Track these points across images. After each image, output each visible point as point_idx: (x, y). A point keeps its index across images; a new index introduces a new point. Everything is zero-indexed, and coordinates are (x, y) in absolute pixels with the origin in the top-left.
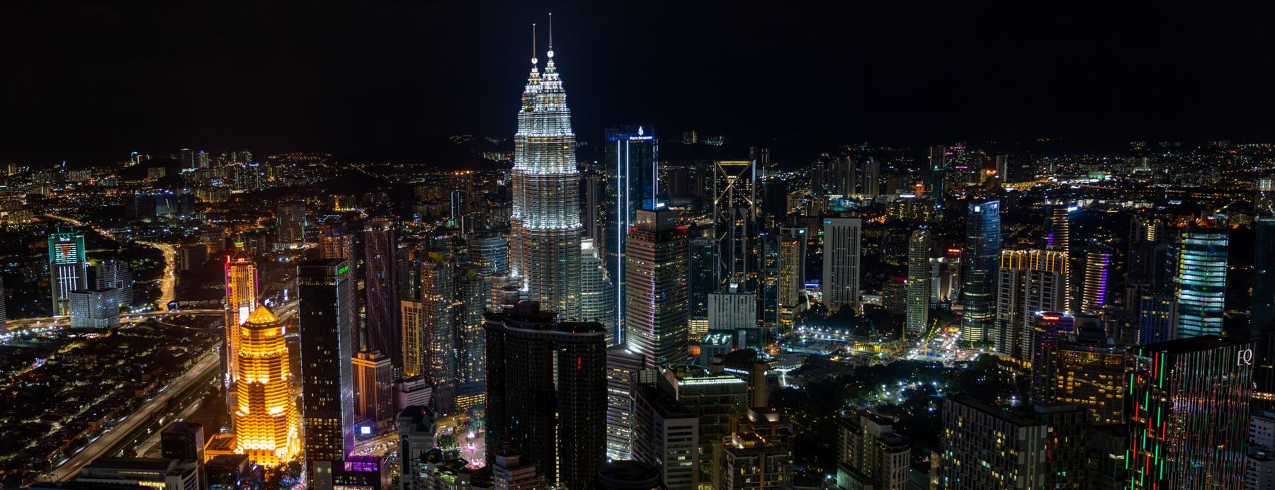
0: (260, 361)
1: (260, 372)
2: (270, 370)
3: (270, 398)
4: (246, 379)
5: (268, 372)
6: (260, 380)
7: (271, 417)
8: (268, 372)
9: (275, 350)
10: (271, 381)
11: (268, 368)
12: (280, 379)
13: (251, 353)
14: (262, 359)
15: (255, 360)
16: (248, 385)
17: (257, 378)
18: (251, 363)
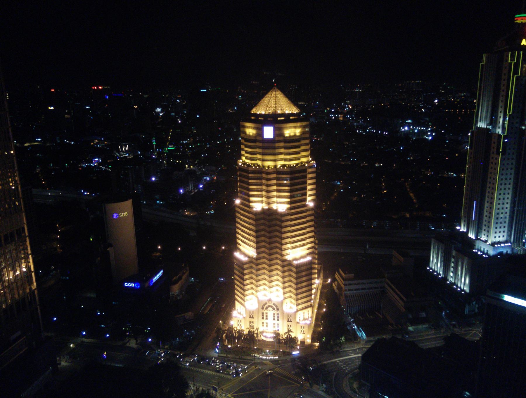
0: (274, 176)
1: (275, 193)
3: (289, 234)
4: (251, 204)
6: (274, 206)
7: (290, 264)
9: (299, 159)
10: (291, 209)
11: (287, 188)
12: (305, 206)
13: (259, 163)
15: (268, 173)
16: (256, 214)
17: (269, 203)
18: (261, 179)
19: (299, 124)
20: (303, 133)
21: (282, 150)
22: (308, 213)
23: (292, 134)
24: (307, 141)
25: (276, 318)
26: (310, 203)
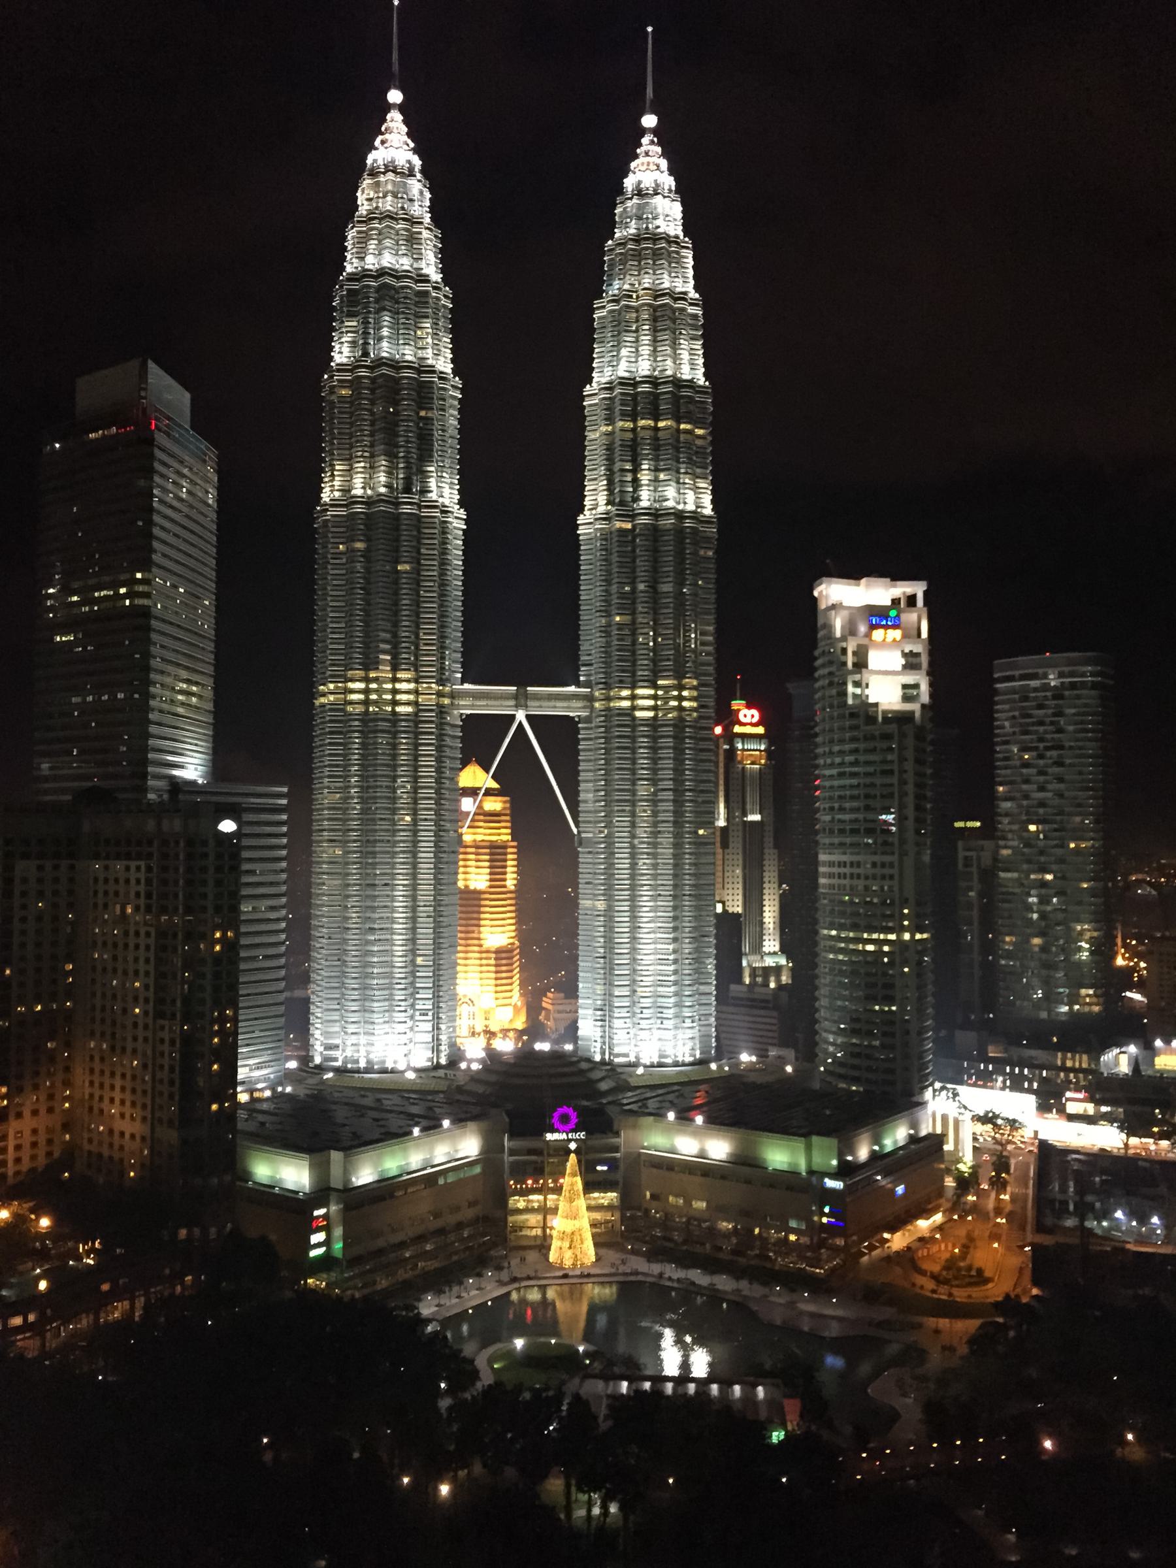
0: (473, 850)
2: (490, 867)
3: (488, 909)
5: (488, 870)
8: (488, 870)
10: (491, 887)
11: (487, 864)
12: (505, 886)
14: (477, 847)
15: (466, 847)
19: (500, 798)
20: (504, 809)
21: (481, 824)
22: (509, 895)
23: (492, 809)
24: (508, 818)
25: (471, 1017)
26: (511, 881)
